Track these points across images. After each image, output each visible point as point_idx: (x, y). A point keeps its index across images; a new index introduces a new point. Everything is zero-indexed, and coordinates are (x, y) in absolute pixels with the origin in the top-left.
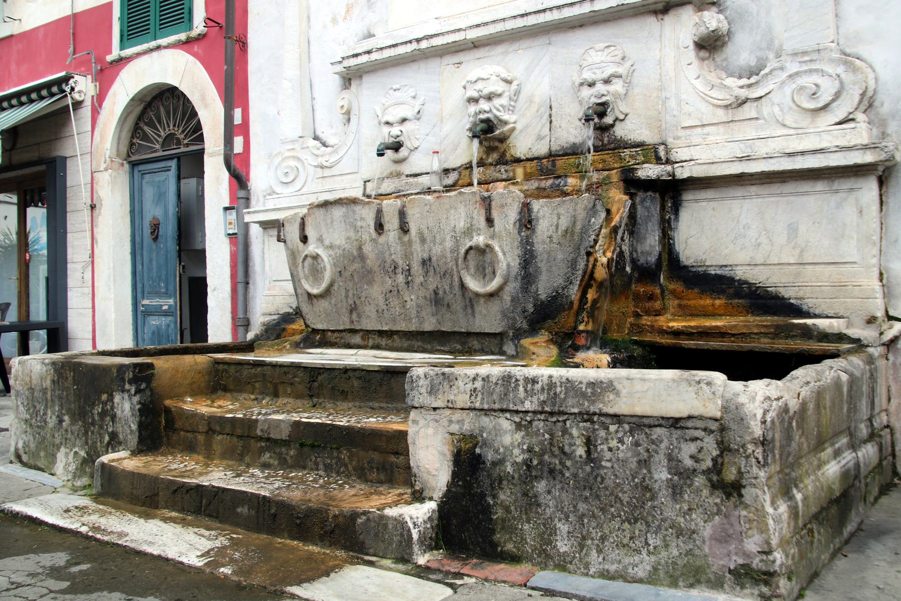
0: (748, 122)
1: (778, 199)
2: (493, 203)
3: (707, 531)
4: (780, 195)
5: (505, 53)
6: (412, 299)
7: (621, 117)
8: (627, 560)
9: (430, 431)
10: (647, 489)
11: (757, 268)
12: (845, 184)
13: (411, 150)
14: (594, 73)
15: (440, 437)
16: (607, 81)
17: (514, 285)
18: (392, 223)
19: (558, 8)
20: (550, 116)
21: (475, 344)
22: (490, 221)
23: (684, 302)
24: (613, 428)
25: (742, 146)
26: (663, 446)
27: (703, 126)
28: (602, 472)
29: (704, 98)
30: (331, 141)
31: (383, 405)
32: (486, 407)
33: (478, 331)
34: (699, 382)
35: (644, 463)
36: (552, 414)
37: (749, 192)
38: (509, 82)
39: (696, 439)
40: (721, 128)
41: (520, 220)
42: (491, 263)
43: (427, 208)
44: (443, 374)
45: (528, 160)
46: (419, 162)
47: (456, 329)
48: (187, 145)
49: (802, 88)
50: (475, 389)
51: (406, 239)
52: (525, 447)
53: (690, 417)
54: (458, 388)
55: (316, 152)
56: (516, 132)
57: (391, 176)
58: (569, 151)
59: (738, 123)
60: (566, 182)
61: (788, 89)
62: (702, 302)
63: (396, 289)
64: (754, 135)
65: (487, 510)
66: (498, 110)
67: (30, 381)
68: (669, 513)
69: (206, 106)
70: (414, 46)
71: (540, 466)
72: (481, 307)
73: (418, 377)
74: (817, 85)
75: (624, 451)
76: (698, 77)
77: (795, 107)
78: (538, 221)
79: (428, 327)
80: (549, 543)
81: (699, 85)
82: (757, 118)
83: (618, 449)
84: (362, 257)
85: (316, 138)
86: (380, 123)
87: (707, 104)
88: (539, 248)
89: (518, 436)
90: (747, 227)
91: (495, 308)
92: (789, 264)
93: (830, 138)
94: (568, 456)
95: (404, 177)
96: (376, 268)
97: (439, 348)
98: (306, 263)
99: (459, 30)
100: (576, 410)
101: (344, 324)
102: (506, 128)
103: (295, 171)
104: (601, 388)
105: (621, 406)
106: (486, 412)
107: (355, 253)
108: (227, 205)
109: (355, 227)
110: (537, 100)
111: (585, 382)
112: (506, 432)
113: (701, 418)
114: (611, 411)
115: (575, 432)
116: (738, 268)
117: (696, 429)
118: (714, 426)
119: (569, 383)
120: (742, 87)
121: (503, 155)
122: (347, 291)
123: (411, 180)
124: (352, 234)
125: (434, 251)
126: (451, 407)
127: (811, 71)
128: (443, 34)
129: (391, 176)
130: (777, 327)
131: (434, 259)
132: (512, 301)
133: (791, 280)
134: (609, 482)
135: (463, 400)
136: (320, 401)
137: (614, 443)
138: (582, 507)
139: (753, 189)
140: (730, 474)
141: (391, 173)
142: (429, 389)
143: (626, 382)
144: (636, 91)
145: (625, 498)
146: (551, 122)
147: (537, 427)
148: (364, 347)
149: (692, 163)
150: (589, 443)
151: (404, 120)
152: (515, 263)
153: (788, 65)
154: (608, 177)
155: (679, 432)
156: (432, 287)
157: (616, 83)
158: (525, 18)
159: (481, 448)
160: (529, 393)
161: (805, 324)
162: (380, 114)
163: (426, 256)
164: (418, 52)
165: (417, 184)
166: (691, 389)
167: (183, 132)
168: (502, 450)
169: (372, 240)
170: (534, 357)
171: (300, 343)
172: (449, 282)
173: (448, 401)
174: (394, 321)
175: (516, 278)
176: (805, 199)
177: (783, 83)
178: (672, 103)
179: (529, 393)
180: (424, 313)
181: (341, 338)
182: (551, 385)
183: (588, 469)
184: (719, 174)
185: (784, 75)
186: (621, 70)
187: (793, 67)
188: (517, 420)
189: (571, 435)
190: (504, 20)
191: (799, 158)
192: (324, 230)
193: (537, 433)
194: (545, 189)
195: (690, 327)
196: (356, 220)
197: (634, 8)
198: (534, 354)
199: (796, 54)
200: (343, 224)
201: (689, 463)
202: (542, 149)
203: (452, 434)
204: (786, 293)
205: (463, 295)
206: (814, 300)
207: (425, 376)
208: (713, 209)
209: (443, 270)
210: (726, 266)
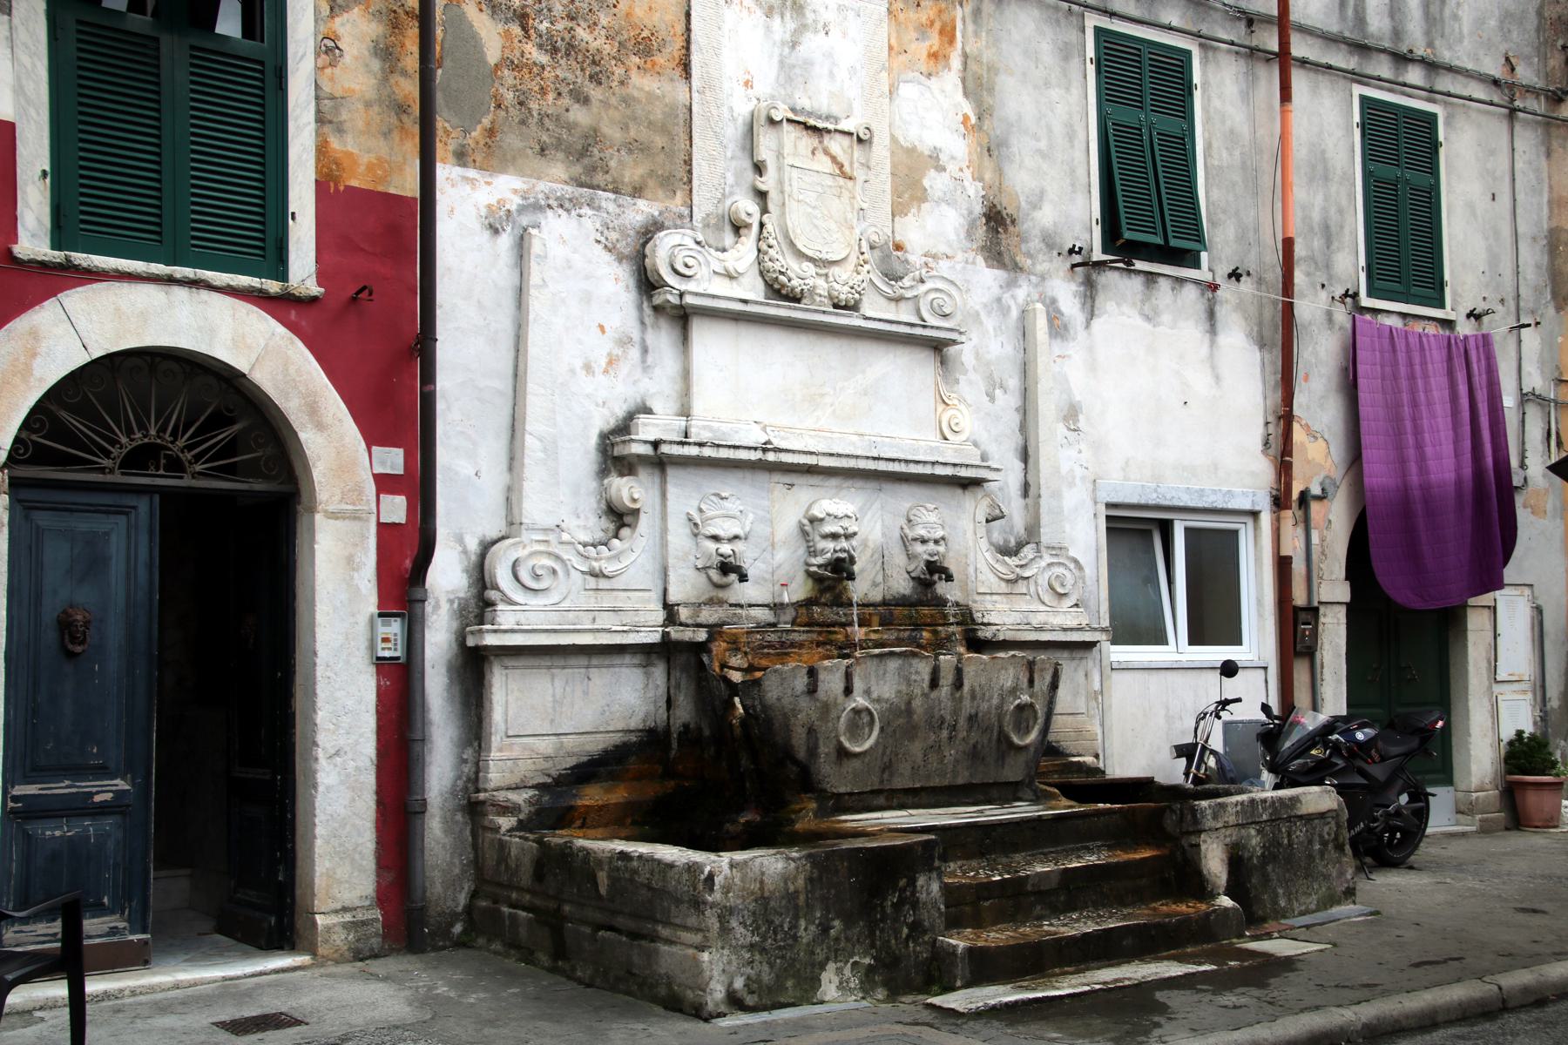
5: (839, 488)
6: (950, 754)
12: (1078, 654)
16: (936, 542)
18: (947, 679)
19: (907, 461)
22: (1031, 682)
29: (992, 569)
35: (1310, 842)
57: (711, 602)
67: (762, 889)
69: (320, 426)
71: (1269, 856)
79: (960, 781)
84: (909, 711)
91: (1022, 758)
94: (1280, 845)
95: (726, 606)
106: (1242, 826)
110: (871, 544)
121: (839, 596)
122: (885, 748)
127: (1060, 564)
128: (793, 452)
129: (711, 602)
135: (1232, 820)
144: (951, 554)
150: (1289, 835)
151: (736, 537)
160: (1264, 809)
165: (748, 617)
167: (129, 432)
169: (925, 695)
174: (928, 777)
178: (971, 570)
182: (1273, 802)
185: (1043, 564)
187: (1047, 559)
192: (873, 682)
202: (876, 596)
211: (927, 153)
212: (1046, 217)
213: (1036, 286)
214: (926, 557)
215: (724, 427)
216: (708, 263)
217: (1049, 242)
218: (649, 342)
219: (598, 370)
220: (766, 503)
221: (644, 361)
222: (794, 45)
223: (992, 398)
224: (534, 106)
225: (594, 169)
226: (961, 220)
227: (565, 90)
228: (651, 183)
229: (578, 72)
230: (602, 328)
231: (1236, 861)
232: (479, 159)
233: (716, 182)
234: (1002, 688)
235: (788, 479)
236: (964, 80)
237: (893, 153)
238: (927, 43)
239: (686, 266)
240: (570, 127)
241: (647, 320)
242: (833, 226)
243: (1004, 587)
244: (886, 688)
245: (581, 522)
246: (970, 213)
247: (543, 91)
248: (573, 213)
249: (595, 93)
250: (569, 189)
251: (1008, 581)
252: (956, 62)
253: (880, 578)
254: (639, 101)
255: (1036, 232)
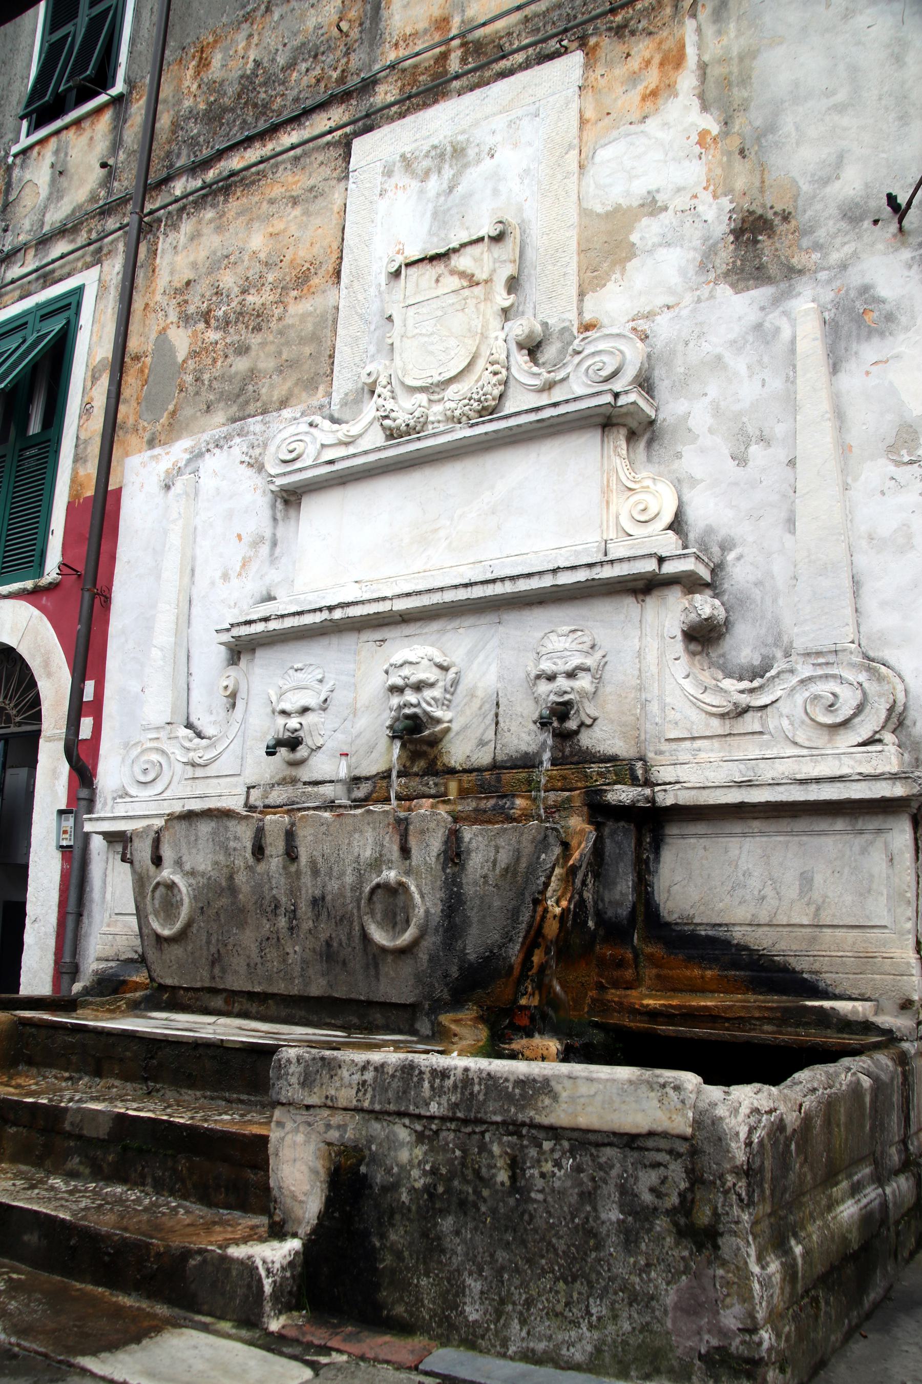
0: (750, 737)
1: (787, 838)
2: (411, 827)
3: (670, 1298)
4: (791, 833)
5: (443, 631)
6: (295, 951)
7: (588, 721)
8: (560, 1336)
9: (300, 1138)
10: (591, 1233)
11: (761, 930)
12: (874, 823)
13: (313, 750)
14: (555, 664)
15: (312, 1147)
16: (571, 675)
17: (434, 939)
18: (275, 846)
19: (513, 578)
20: (497, 715)
21: (378, 1017)
22: (405, 851)
23: (665, 972)
24: (547, 1145)
25: (742, 767)
26: (614, 1173)
27: (693, 738)
28: (531, 1207)
29: (695, 702)
30: (209, 731)
31: (244, 1097)
32: (377, 1107)
33: (382, 1000)
34: (664, 1086)
35: (589, 1197)
36: (466, 1122)
37: (750, 827)
38: (444, 669)
39: (656, 1165)
40: (716, 743)
41: (445, 852)
42: (404, 908)
43: (324, 828)
44: (323, 1059)
45: (465, 771)
46: (323, 766)
47: (353, 996)
48: (20, 724)
49: (816, 698)
50: (365, 1082)
51: (293, 869)
52: (428, 1167)
53: (651, 1134)
54: (342, 1079)
55: (187, 744)
56: (452, 734)
57: (283, 782)
58: (519, 763)
59: (737, 738)
60: (513, 803)
61: (800, 697)
62: (688, 973)
63: (275, 936)
64: (755, 753)
65: (372, 1255)
66: (429, 704)
68: (620, 1270)
69: (49, 675)
70: (325, 615)
72: (388, 968)
73: (289, 1061)
74: (834, 695)
75: (561, 1177)
76: (688, 676)
77: (809, 721)
78: (469, 854)
79: (315, 991)
80: (455, 1306)
81: (687, 684)
82: (761, 733)
83: (554, 1175)
84: (232, 889)
85: (189, 726)
86: (273, 712)
87: (698, 711)
88: (469, 890)
89: (419, 1152)
90: (747, 874)
91: (407, 969)
92: (802, 926)
93: (852, 763)
96: (250, 907)
97: (328, 1020)
98: (158, 894)
99: (384, 599)
100: (498, 1118)
101: (202, 980)
102: (439, 728)
103: (157, 768)
104: (534, 1089)
105: (560, 1115)
106: (377, 1115)
107: (224, 884)
108: (64, 807)
109: (227, 849)
110: (480, 693)
111: (512, 1078)
112: (402, 1145)
113: (665, 1135)
114: (546, 1121)
115: (496, 1149)
116: (737, 928)
117: (658, 1150)
118: (683, 1148)
119: (490, 1078)
120: (742, 692)
121: (433, 762)
122: (209, 935)
123: (309, 789)
124: (221, 858)
125: (329, 888)
126: (330, 1105)
127: (826, 677)
128: (362, 602)
129: (283, 782)
130: (786, 1010)
131: (329, 898)
132: (430, 960)
133: (804, 947)
134: (539, 1222)
135: (346, 1096)
136: (158, 1086)
137: (548, 1167)
138: (502, 1256)
139: (756, 825)
140: (703, 1216)
141: (284, 779)
142: (302, 1079)
143: (568, 1083)
144: (609, 689)
145: (561, 1246)
146: (497, 723)
147: (445, 1139)
148: (227, 1014)
149: (678, 786)
150: (515, 1165)
151: (305, 710)
152: (436, 910)
153: (799, 667)
154: (569, 800)
155: (636, 1154)
156: (323, 936)
157: (583, 678)
158: (469, 589)
159: (368, 1165)
160: (438, 1092)
161: (821, 1007)
162: (274, 699)
163: (318, 893)
164: (330, 624)
166: (652, 1094)
168: (395, 1170)
169: (249, 868)
170: (455, 1039)
171: (140, 1003)
172: (346, 930)
173: (327, 1097)
174: (270, 979)
175: (436, 930)
176: (823, 840)
177: (793, 689)
178: (654, 708)
179: (438, 1092)
180: (311, 971)
181: (197, 999)
183: (511, 1201)
184: (711, 802)
185: (794, 680)
186: (589, 662)
187: (805, 671)
188: (419, 1128)
189: (491, 1153)
190: (442, 589)
191: (814, 787)
192: (184, 850)
193: (445, 1149)
194: (485, 811)
195: (671, 1006)
196: (228, 839)
197: (607, 584)
198: (455, 1035)
199: (809, 654)
200: (211, 843)
201: (647, 1198)
202: (484, 758)
203: (329, 1144)
204: (799, 965)
205: (365, 950)
206: (834, 976)
207: (298, 1060)
208: (705, 848)
209: (340, 913)
210: (720, 925)
211: (635, 204)
212: (851, 183)
213: (829, 281)
214: (553, 698)
215: (311, 597)
216: (315, 439)
217: (852, 215)
218: (278, 535)
219: (233, 575)
220: (352, 666)
221: (272, 554)
222: (451, 189)
223: (741, 459)
224: (206, 377)
225: (247, 403)
226: (692, 254)
227: (230, 351)
228: (296, 391)
229: (243, 331)
230: (239, 537)
231: (348, 1179)
232: (163, 438)
233: (357, 359)
234: (357, 860)
235: (378, 635)
236: (702, 97)
237: (583, 228)
238: (640, 88)
239: (291, 452)
240: (230, 380)
241: (279, 516)
242: (452, 342)
243: (716, 726)
244: (200, 858)
245: (213, 718)
246: (706, 239)
247: (215, 361)
248: (225, 447)
249: (255, 340)
250: (225, 429)
251: (723, 716)
252: (687, 81)
253: (490, 734)
254: (293, 326)
255: (833, 210)
